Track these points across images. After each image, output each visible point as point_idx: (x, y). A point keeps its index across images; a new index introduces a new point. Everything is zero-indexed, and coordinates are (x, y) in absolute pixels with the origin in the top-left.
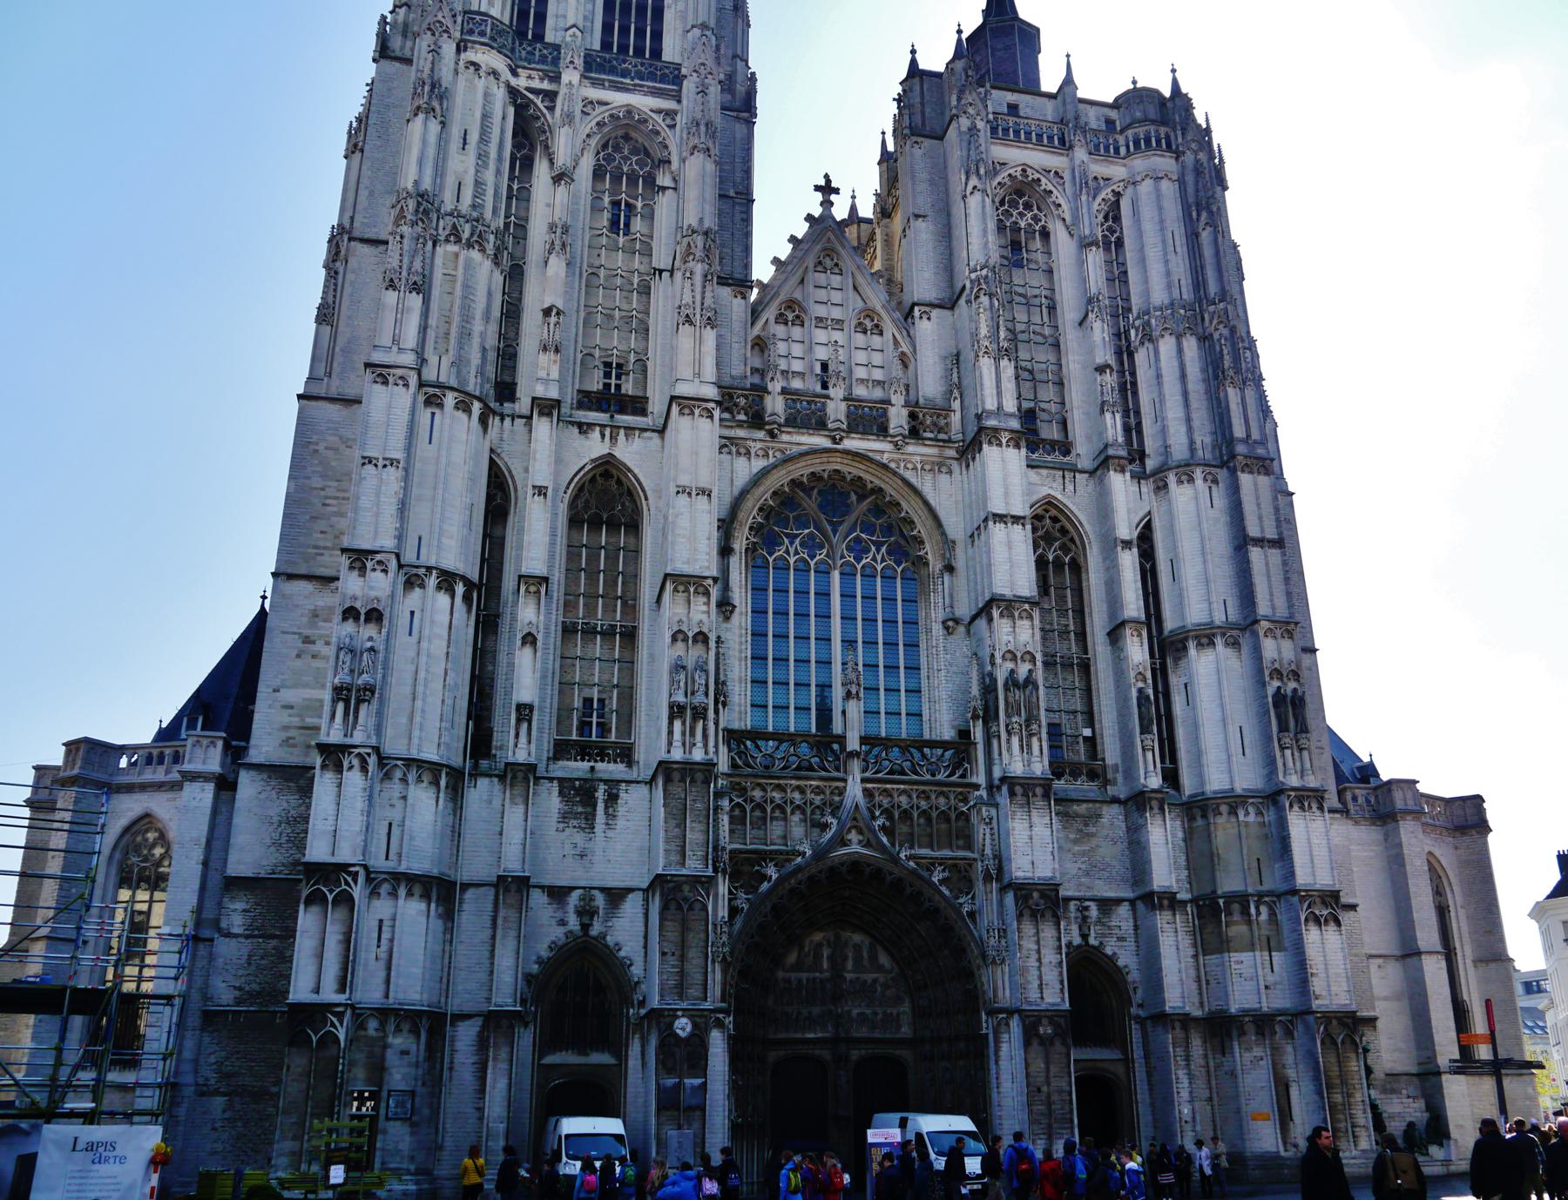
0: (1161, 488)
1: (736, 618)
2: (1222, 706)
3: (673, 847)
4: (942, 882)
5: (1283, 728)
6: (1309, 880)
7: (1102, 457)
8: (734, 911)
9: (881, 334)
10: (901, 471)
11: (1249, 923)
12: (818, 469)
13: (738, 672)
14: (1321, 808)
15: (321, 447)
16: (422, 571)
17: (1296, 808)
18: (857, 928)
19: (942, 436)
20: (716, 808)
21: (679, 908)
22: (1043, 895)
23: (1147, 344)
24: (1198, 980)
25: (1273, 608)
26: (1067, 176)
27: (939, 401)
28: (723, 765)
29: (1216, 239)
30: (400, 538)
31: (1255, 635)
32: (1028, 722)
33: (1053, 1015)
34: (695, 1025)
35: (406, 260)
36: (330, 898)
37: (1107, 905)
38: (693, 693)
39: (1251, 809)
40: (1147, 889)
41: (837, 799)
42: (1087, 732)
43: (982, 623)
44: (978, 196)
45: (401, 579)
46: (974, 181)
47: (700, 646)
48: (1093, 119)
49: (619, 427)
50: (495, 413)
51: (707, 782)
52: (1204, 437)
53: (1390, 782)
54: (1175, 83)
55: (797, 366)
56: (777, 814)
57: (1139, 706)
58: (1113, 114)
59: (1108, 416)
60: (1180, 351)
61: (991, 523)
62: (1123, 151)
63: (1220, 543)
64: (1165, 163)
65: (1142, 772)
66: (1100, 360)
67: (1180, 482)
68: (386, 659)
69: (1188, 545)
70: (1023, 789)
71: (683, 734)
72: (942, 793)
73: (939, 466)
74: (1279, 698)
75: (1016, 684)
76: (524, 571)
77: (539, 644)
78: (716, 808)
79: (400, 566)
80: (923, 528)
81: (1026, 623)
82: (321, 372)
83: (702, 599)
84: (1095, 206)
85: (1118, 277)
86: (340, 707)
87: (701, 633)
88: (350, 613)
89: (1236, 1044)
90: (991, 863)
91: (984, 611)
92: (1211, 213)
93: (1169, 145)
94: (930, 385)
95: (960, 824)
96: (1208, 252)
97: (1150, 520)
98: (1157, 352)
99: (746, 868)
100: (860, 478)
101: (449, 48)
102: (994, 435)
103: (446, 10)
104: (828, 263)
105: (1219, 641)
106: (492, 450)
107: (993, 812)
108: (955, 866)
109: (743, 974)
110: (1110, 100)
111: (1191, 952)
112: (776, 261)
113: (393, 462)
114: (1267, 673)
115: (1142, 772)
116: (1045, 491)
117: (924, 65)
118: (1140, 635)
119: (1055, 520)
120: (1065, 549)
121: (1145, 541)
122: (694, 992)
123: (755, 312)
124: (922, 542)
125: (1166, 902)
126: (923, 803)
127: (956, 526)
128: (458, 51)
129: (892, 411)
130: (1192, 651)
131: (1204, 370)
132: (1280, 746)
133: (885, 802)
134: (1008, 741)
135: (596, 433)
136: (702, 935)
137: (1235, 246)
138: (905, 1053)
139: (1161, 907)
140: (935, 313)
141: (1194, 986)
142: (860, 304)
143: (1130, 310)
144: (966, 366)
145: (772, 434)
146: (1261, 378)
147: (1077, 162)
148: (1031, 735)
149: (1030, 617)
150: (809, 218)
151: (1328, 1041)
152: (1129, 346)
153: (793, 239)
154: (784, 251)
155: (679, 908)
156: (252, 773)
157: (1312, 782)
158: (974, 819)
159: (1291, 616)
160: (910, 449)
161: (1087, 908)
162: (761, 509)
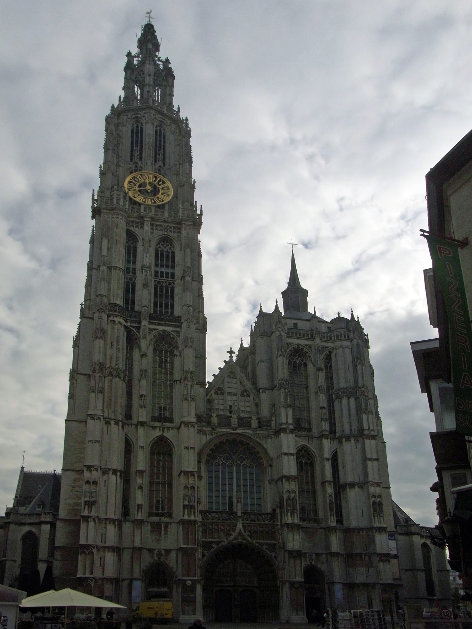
5: (375, 511)
7: (321, 434)
13: (203, 494)
14: (386, 532)
17: (378, 532)
23: (338, 399)
38: (190, 502)
49: (165, 427)
50: (126, 424)
51: (195, 524)
52: (355, 427)
67: (346, 441)
70: (291, 527)
74: (374, 503)
75: (290, 500)
76: (138, 469)
77: (143, 488)
81: (294, 483)
85: (329, 378)
106: (126, 435)
121: (334, 458)
132: (374, 515)
135: (158, 429)
143: (333, 388)
148: (294, 513)
149: (295, 481)
152: (332, 399)
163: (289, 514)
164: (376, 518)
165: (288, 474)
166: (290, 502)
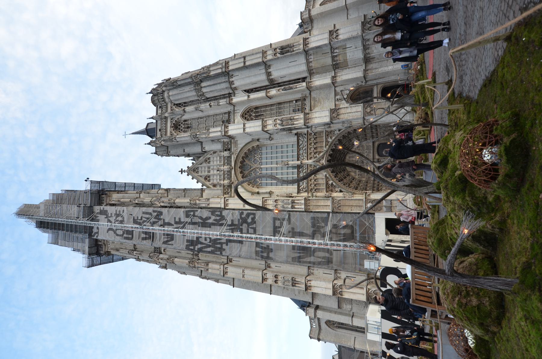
0: (236, 89)
1: (273, 190)
2: (285, 68)
3: (325, 208)
4: (331, 138)
5: (288, 51)
6: (327, 39)
8: (341, 191)
9: (210, 158)
10: (238, 152)
11: (339, 55)
12: (239, 172)
15: (244, 283)
16: (267, 264)
17: (308, 46)
18: (345, 158)
19: (229, 143)
20: (316, 197)
21: (340, 206)
22: (334, 113)
24: (355, 67)
25: (259, 57)
26: (172, 117)
27: (222, 144)
28: (305, 194)
29: (180, 80)
30: (259, 269)
31: (266, 61)
32: (291, 120)
33: (365, 108)
34: (369, 202)
35: (202, 267)
36: (341, 290)
37: (336, 95)
39: (310, 58)
40: (332, 84)
41: (312, 166)
42: (294, 102)
43: (269, 132)
44: (176, 139)
45: (268, 269)
46: (174, 140)
47: (278, 201)
48: (159, 112)
51: (309, 200)
52: (223, 79)
53: (301, 19)
54: (150, 93)
55: (218, 177)
56: (316, 181)
57: (286, 90)
58: (159, 107)
59: (220, 104)
60: (205, 87)
61: (246, 132)
62: (165, 104)
63: (246, 73)
64: (166, 95)
65: (302, 88)
66: (209, 107)
67: (234, 84)
68: (286, 273)
69: (248, 81)
70: (306, 119)
71: (298, 205)
72: (310, 140)
73: (236, 143)
74: (282, 53)
75: (282, 124)
78: (316, 197)
79: (266, 269)
80: (250, 147)
81: (268, 122)
82: (228, 282)
83: (268, 201)
84: (177, 110)
85: (192, 103)
86: (296, 285)
87: (275, 201)
88: (276, 282)
89: (372, 55)
90: (326, 127)
91: (266, 132)
92: (174, 82)
93: (161, 94)
94: (218, 147)
95: (317, 134)
96: (182, 82)
97: (244, 91)
98: (206, 92)
99: (330, 188)
100: (240, 162)
101: (161, 256)
102: (226, 132)
103: (154, 256)
104: (197, 170)
105: (269, 70)
107: (313, 127)
108: (327, 135)
109: (356, 189)
110: (155, 108)
111: (348, 70)
112: (197, 182)
113: (243, 271)
114: (275, 57)
115: (302, 88)
116: (239, 117)
117: (154, 151)
118: (269, 91)
119: (246, 114)
120: (252, 111)
122: (361, 202)
123: (208, 187)
124: (253, 147)
125: (335, 79)
126: (313, 144)
127: (249, 139)
128: (162, 253)
129: (225, 155)
130: (272, 77)
131: (208, 80)
133: (313, 154)
134: (296, 124)
136: (347, 201)
137: (182, 74)
138: (376, 144)
139: (335, 80)
140: (203, 146)
141: (357, 68)
142: (204, 163)
144: (213, 139)
145: (232, 183)
146: (210, 65)
147: (168, 115)
148: (294, 119)
149: (266, 121)
150: (188, 175)
151: (370, 29)
153: (193, 179)
154: (195, 180)
155: (340, 206)
156: (314, 301)
157: (302, 41)
158: (315, 131)
159: (261, 52)
160: (233, 150)
161: (337, 99)
162: (249, 185)
163: (295, 123)
164: (294, 49)
165: (261, 127)
166: (284, 123)
